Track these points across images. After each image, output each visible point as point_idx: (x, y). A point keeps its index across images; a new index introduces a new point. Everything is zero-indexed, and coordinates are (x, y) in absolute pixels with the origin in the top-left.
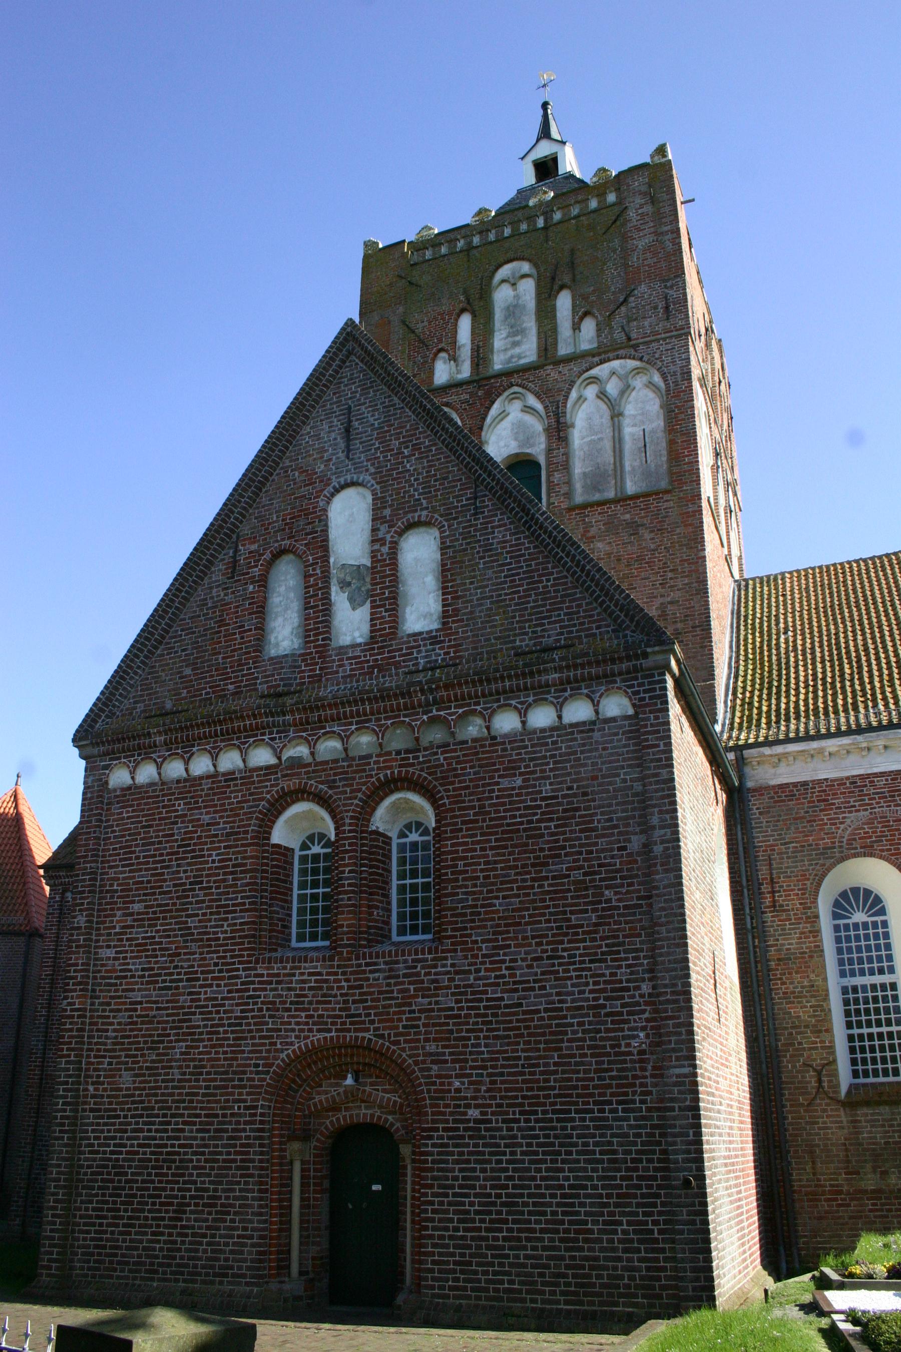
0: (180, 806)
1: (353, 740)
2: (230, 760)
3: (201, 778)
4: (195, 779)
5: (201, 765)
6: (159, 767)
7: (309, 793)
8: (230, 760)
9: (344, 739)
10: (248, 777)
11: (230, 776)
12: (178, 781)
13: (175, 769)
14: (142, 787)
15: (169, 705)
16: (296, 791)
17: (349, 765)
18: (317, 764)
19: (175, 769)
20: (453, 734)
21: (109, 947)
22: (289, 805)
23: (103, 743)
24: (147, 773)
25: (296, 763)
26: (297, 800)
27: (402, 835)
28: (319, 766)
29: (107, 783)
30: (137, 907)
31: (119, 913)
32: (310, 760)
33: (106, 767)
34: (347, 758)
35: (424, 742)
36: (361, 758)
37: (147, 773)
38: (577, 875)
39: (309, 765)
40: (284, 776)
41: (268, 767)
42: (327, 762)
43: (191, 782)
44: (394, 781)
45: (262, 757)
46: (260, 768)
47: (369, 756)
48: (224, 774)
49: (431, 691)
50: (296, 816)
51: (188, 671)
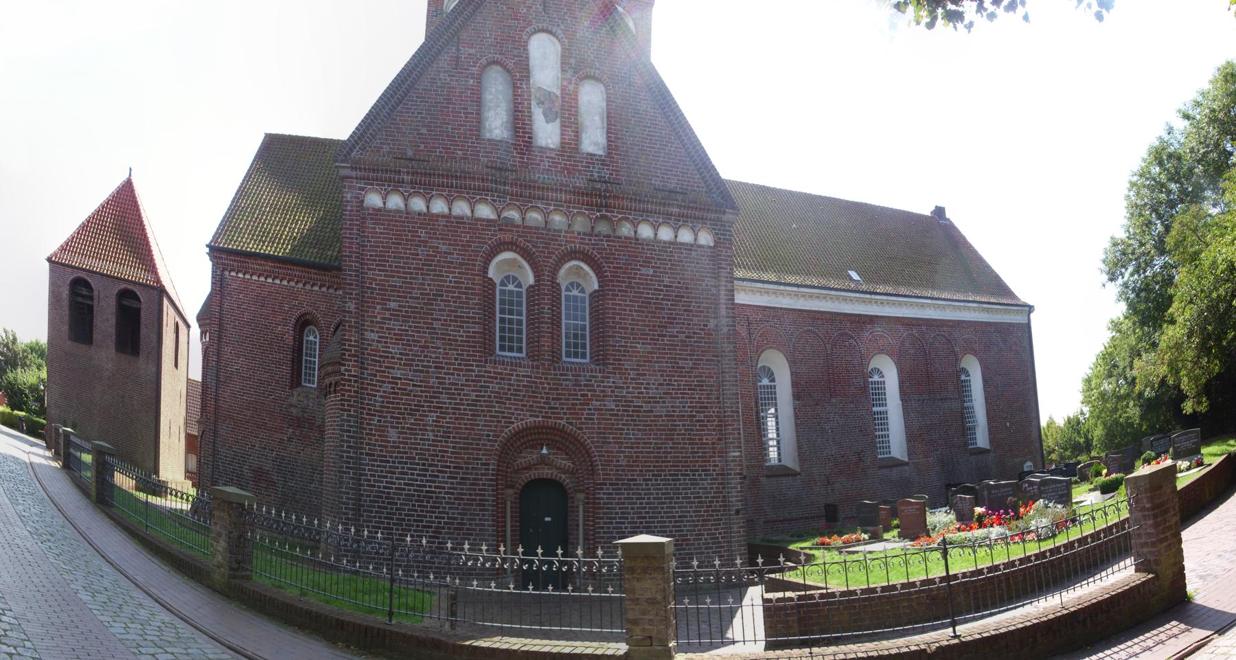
0: (422, 234)
1: (551, 217)
2: (461, 208)
3: (437, 215)
4: (433, 215)
5: (439, 206)
6: (406, 200)
7: (517, 246)
8: (461, 208)
9: (546, 215)
10: (476, 223)
11: (460, 220)
12: (419, 214)
13: (418, 204)
14: (390, 211)
15: (410, 153)
16: (508, 243)
17: (547, 234)
18: (525, 227)
19: (418, 204)
20: (614, 231)
21: (372, 331)
22: (501, 251)
23: (360, 169)
24: (395, 202)
25: (509, 223)
26: (508, 250)
27: (567, 289)
28: (526, 229)
29: (363, 201)
30: (393, 305)
31: (379, 307)
32: (520, 223)
33: (362, 189)
34: (545, 228)
35: (596, 231)
36: (555, 230)
37: (395, 202)
38: (682, 337)
39: (518, 226)
40: (500, 230)
41: (489, 221)
42: (530, 228)
43: (429, 218)
44: (575, 252)
45: (485, 211)
46: (483, 220)
47: (560, 231)
48: (455, 218)
49: (605, 197)
50: (505, 261)
51: (424, 131)
